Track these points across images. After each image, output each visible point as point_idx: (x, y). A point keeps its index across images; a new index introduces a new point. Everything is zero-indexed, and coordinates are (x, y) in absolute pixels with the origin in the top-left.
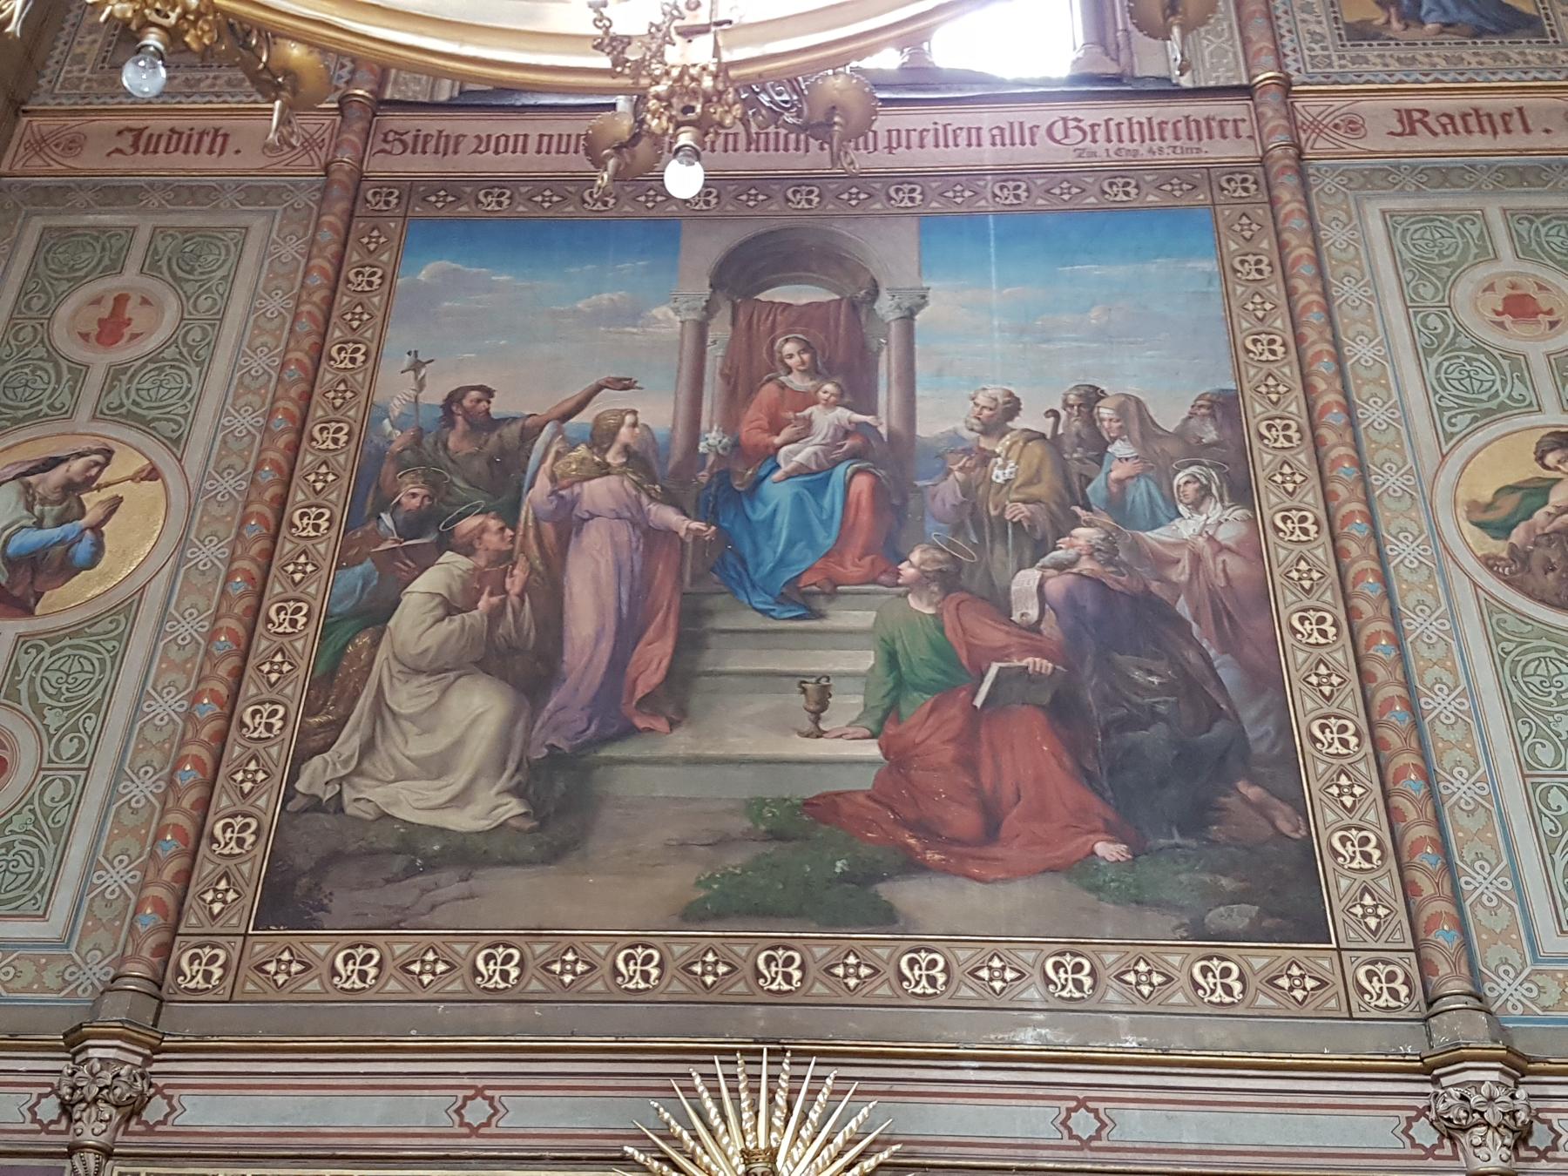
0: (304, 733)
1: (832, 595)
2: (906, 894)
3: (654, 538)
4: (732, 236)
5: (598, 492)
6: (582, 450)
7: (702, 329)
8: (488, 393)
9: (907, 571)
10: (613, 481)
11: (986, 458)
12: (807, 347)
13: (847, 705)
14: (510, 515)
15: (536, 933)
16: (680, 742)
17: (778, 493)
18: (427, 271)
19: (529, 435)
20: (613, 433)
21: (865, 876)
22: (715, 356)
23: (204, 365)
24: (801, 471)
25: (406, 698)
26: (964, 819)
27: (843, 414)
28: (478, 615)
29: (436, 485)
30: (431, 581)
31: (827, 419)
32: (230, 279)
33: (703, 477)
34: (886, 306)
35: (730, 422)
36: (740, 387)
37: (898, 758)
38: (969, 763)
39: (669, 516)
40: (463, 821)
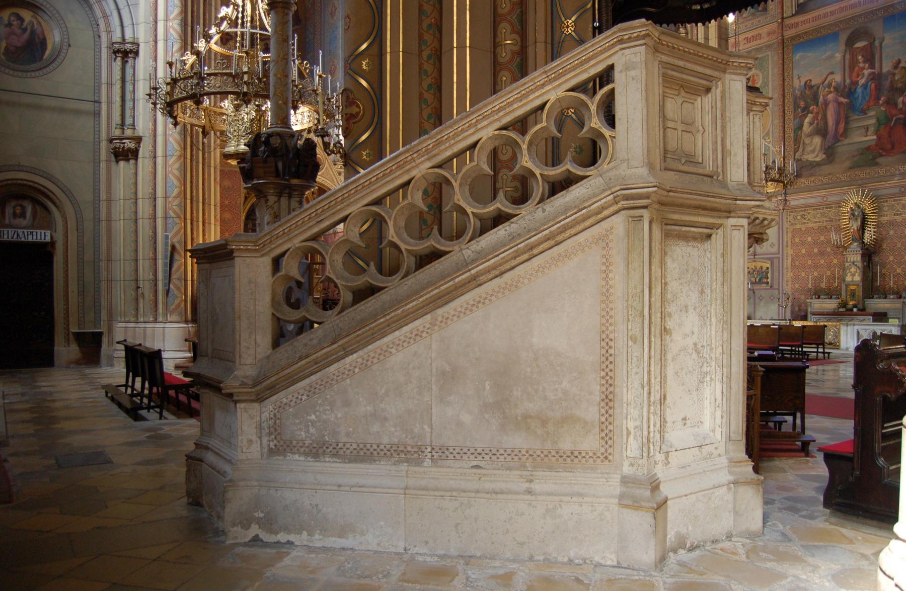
0: (795, 149)
1: (868, 110)
2: (880, 160)
3: (840, 104)
4: (849, 32)
5: (830, 97)
6: (827, 89)
7: (844, 57)
8: (810, 80)
9: (881, 102)
10: (832, 94)
11: (894, 74)
12: (863, 56)
13: (871, 129)
14: (817, 105)
15: (829, 174)
16: (846, 141)
17: (859, 90)
18: (797, 56)
19: (818, 88)
20: (831, 84)
21: (874, 158)
22: (847, 62)
23: (768, 86)
24: (863, 85)
25: (807, 141)
26: (889, 146)
28: (815, 125)
29: (805, 101)
30: (807, 120)
31: (866, 72)
32: (768, 67)
33: (847, 90)
34: (877, 43)
35: (850, 77)
36: (852, 68)
37: (879, 138)
38: (890, 136)
39: (842, 99)
40: (818, 159)
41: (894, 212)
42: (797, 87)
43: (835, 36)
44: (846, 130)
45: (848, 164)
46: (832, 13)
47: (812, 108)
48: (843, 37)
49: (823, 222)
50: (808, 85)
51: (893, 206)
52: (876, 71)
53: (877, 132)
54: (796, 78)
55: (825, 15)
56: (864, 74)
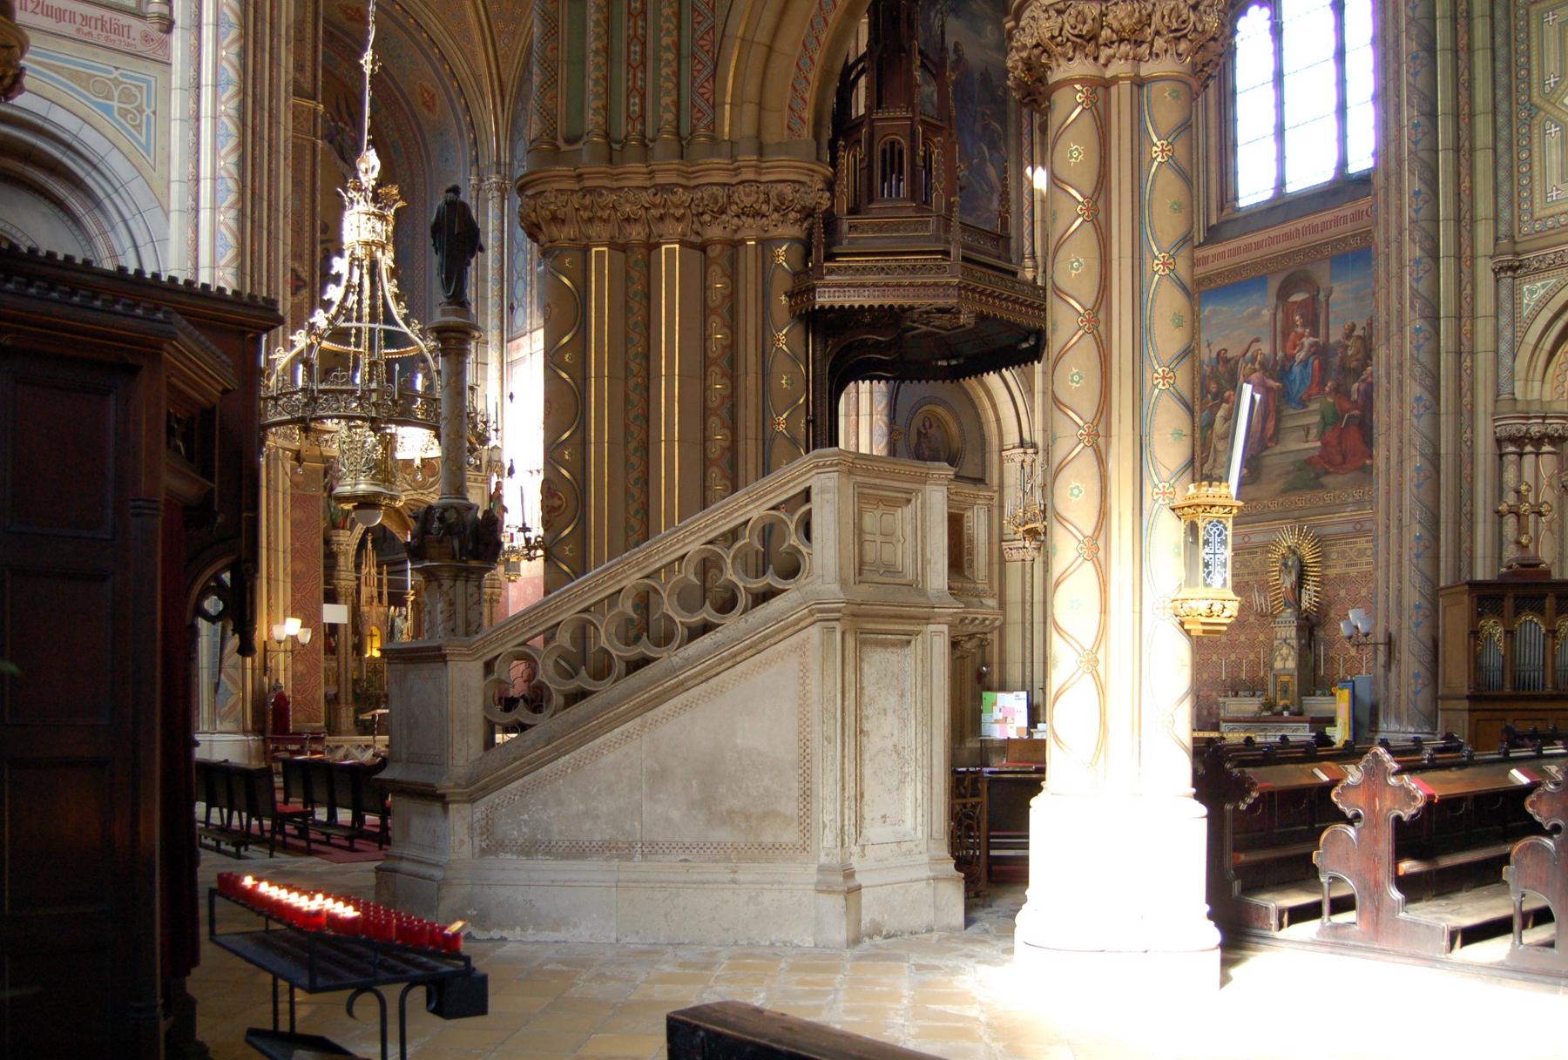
1: (1310, 400)
2: (1326, 480)
4: (1282, 276)
7: (1275, 314)
8: (1226, 350)
9: (1327, 389)
11: (1346, 347)
12: (1302, 317)
13: (1314, 431)
15: (1253, 500)
16: (1278, 449)
17: (1296, 369)
21: (1317, 477)
24: (1302, 361)
26: (1339, 459)
27: (1312, 339)
29: (1218, 383)
31: (1307, 341)
34: (1322, 296)
35: (1284, 348)
36: (1286, 335)
37: (1325, 445)
38: (1340, 444)
39: (1272, 383)
41: (1346, 562)
42: (1206, 360)
43: (1260, 282)
44: (1277, 429)
45: (1279, 484)
46: (1258, 245)
47: (1227, 394)
48: (1274, 285)
49: (1243, 575)
50: (1222, 358)
51: (1345, 552)
52: (1321, 340)
53: (1322, 436)
54: (1204, 345)
55: (1248, 248)
56: (1303, 344)
